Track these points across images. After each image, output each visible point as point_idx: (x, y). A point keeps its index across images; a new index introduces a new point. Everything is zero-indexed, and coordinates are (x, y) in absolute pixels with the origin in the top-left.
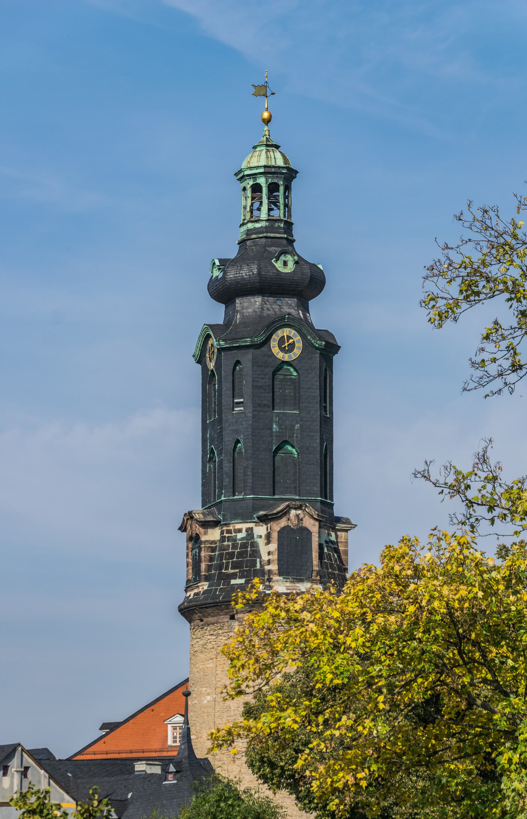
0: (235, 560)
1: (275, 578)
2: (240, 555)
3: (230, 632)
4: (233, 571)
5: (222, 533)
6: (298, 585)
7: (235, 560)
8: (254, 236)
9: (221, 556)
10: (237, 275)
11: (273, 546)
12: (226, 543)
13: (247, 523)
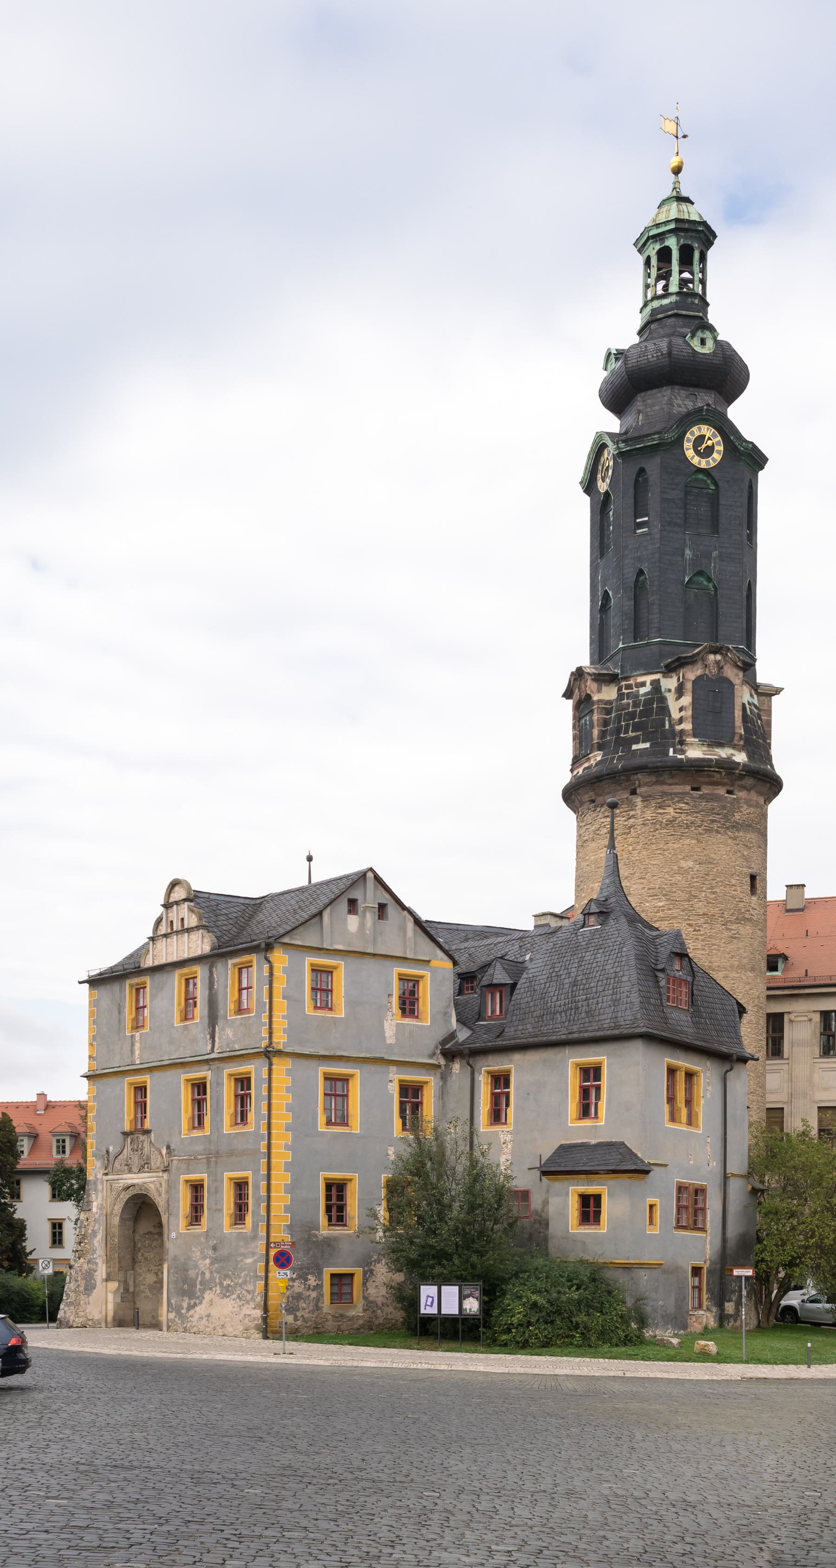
3: (630, 810)
4: (634, 734)
6: (717, 750)
8: (660, 316)
9: (619, 718)
10: (641, 359)
12: (625, 701)
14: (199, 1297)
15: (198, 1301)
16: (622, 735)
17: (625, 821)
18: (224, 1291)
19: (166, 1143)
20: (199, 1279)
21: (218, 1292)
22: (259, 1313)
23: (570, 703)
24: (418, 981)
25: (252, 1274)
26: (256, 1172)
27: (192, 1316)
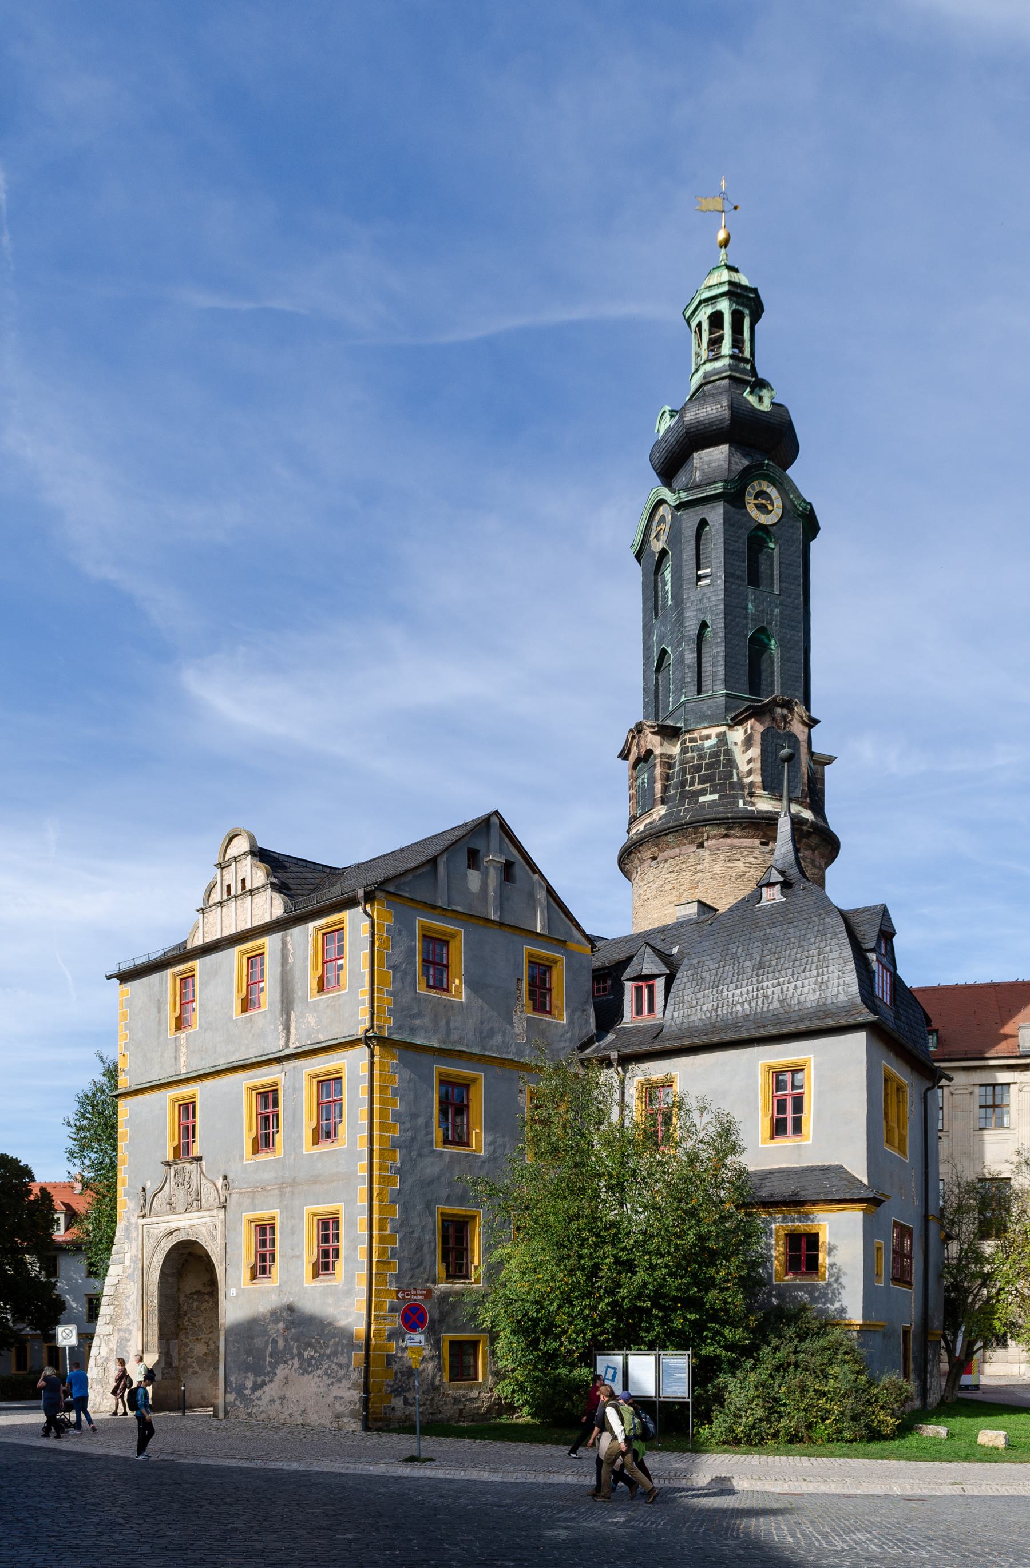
0: (703, 772)
1: (759, 791)
2: (709, 766)
5: (684, 742)
7: (703, 772)
9: (683, 771)
11: (755, 752)
12: (689, 754)
13: (718, 726)
14: (269, 1373)
15: (267, 1379)
16: (687, 788)
17: (693, 875)
18: (305, 1365)
19: (222, 1173)
20: (270, 1349)
21: (296, 1365)
22: (356, 1395)
23: (627, 764)
24: (550, 967)
25: (345, 1342)
26: (350, 1202)
27: (259, 1399)
